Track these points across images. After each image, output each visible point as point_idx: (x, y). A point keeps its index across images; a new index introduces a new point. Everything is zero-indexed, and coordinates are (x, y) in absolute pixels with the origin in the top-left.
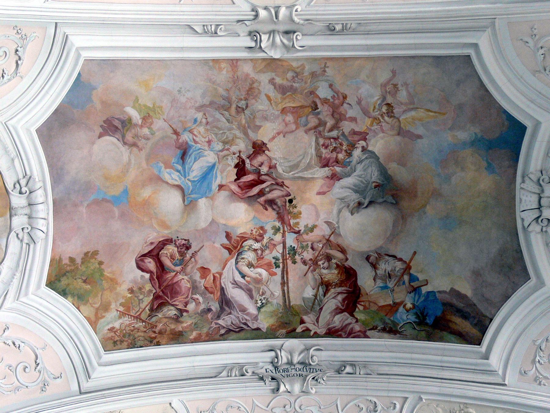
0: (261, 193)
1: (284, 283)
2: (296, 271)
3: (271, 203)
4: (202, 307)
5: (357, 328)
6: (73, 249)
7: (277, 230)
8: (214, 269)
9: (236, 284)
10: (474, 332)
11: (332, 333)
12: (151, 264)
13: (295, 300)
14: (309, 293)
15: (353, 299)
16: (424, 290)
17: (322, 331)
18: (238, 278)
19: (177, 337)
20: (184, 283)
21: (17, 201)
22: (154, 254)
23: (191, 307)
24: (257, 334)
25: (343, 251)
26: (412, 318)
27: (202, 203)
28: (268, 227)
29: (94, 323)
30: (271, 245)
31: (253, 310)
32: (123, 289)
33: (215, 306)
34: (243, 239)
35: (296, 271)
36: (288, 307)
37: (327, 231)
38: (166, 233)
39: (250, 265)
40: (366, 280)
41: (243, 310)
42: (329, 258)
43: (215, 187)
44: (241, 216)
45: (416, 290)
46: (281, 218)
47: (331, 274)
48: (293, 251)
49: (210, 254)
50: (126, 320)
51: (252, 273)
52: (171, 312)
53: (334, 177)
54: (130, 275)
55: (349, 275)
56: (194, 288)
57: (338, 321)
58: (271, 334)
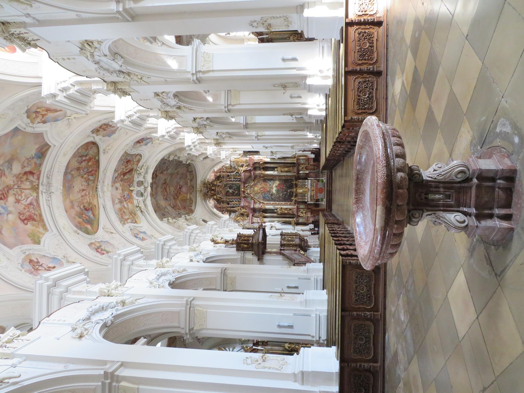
0: (6, 194)
1: (25, 189)
2: (23, 186)
3: (8, 191)
4: (32, 209)
5: (38, 173)
6: (29, 240)
7: (13, 190)
8: (23, 206)
9: (26, 201)
10: (47, 147)
11: (38, 179)
12: (26, 222)
13: (30, 187)
14: (28, 183)
15: (31, 173)
16: (34, 156)
17: (38, 181)
18: (25, 200)
19: (41, 215)
20: (28, 214)
21: (27, 253)
22: (23, 221)
23: (33, 212)
24: (38, 196)
25: (20, 174)
26: (39, 160)
27: (10, 209)
28: (13, 192)
29: (44, 234)
30: (17, 192)
31: (32, 197)
32: (34, 228)
33: (32, 206)
34: (16, 199)
35: (23, 186)
36: (31, 189)
37: (15, 178)
38: (18, 218)
39: (22, 197)
40: (27, 169)
41: (32, 199)
42: (21, 178)
43: (5, 206)
44: (11, 199)
45: (33, 158)
46: (11, 189)
47: (25, 177)
48: (18, 186)
49: (21, 207)
50: (40, 227)
51: (23, 197)
52: (35, 217)
53: (4, 174)
54: (29, 226)
55: (26, 173)
56: (29, 211)
57: (36, 177)
58: (38, 193)
